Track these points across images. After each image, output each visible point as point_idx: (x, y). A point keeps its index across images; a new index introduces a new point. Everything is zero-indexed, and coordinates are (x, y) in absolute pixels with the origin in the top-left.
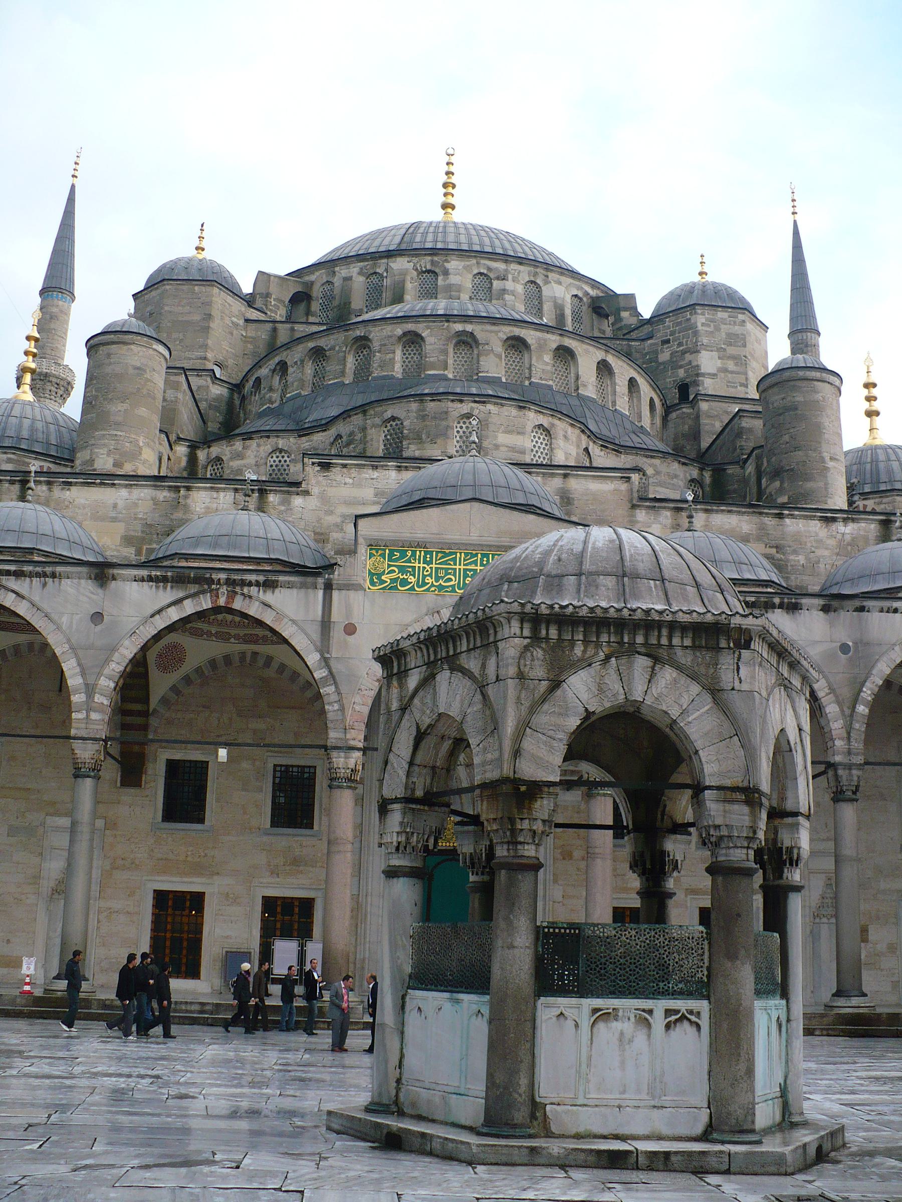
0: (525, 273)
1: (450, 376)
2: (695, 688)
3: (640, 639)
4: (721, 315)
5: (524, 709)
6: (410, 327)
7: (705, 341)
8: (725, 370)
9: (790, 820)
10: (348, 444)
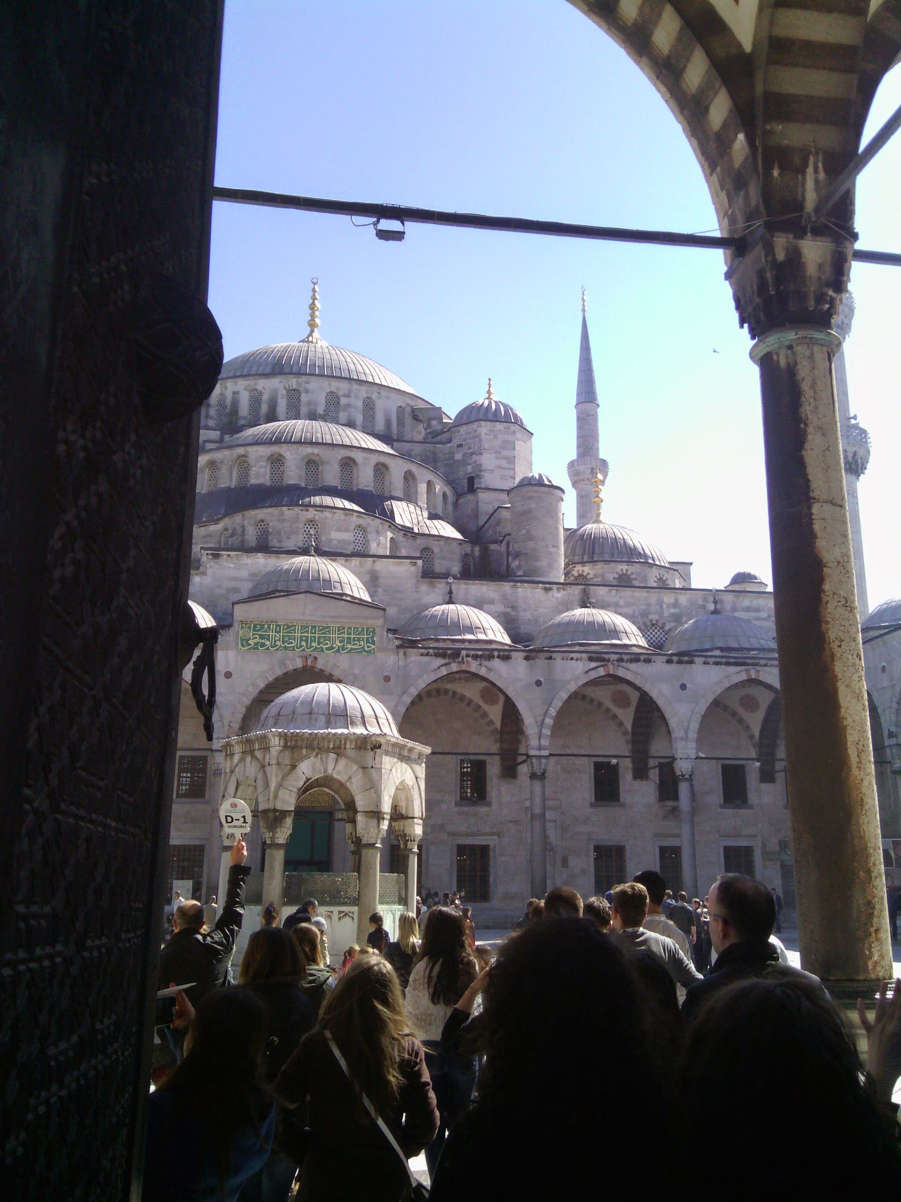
0: (363, 391)
1: (303, 485)
2: (355, 767)
3: (331, 746)
4: (499, 426)
5: (280, 777)
6: (275, 449)
7: (486, 445)
8: (500, 467)
9: (410, 820)
10: (232, 535)
